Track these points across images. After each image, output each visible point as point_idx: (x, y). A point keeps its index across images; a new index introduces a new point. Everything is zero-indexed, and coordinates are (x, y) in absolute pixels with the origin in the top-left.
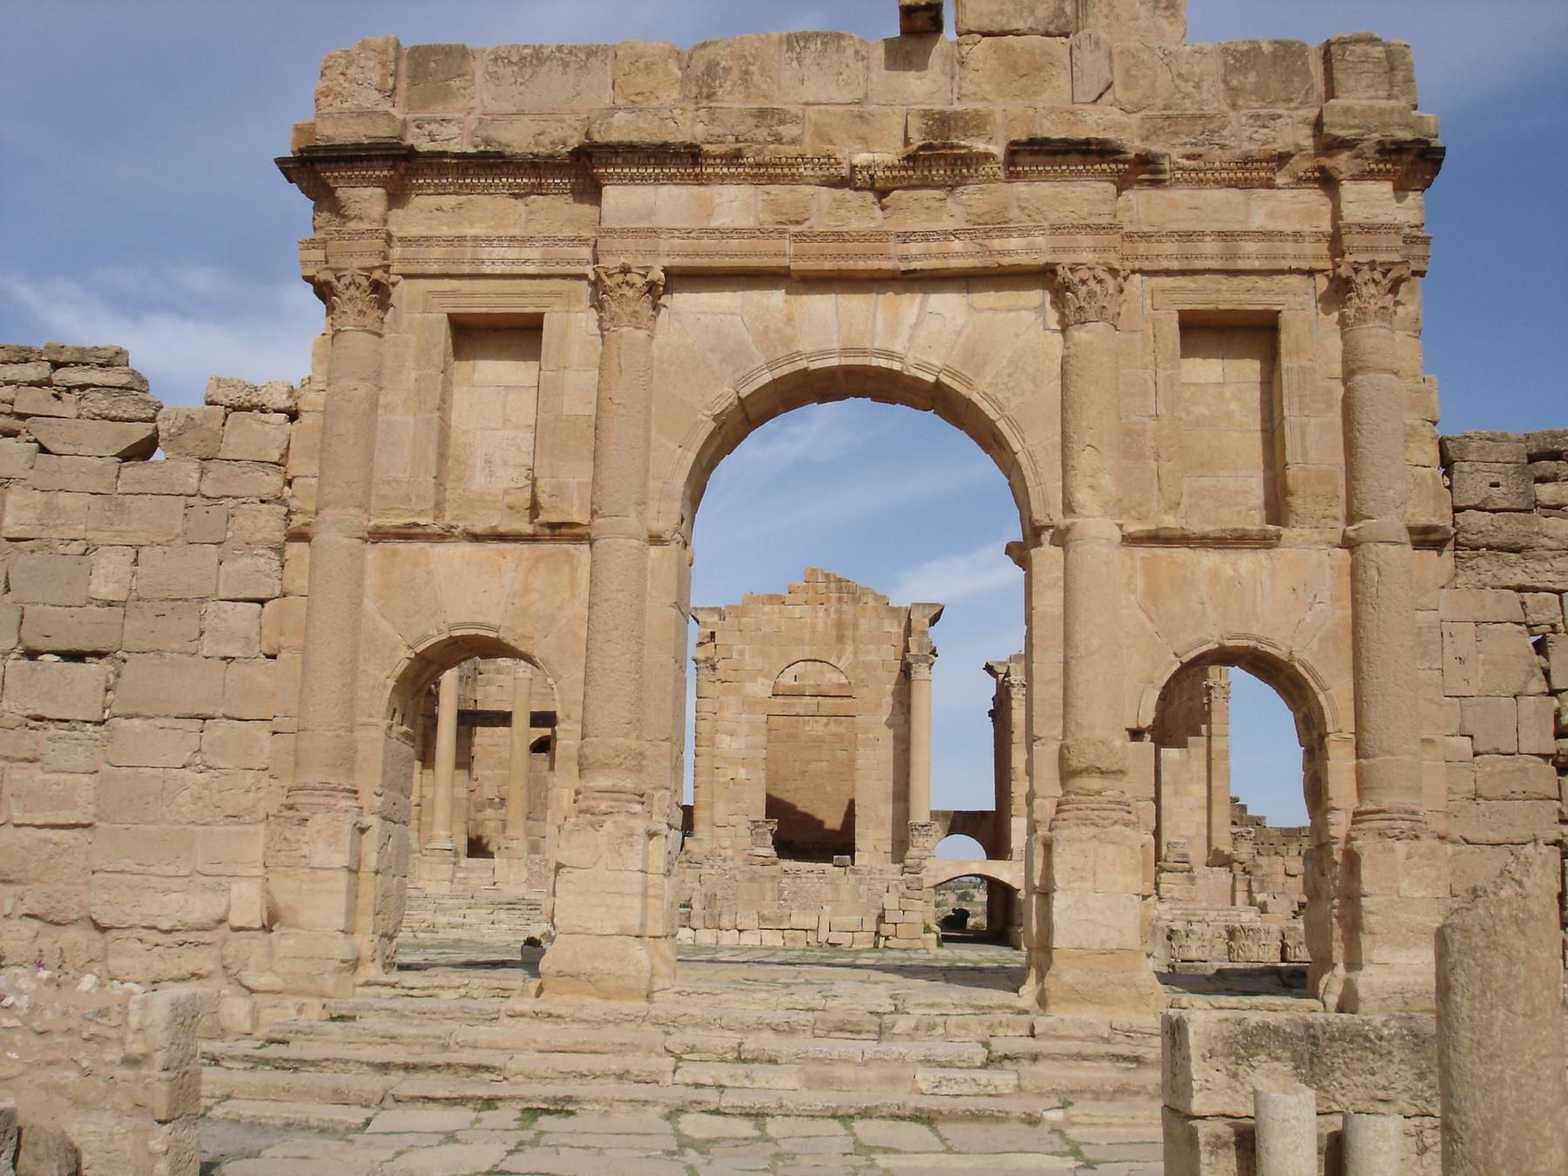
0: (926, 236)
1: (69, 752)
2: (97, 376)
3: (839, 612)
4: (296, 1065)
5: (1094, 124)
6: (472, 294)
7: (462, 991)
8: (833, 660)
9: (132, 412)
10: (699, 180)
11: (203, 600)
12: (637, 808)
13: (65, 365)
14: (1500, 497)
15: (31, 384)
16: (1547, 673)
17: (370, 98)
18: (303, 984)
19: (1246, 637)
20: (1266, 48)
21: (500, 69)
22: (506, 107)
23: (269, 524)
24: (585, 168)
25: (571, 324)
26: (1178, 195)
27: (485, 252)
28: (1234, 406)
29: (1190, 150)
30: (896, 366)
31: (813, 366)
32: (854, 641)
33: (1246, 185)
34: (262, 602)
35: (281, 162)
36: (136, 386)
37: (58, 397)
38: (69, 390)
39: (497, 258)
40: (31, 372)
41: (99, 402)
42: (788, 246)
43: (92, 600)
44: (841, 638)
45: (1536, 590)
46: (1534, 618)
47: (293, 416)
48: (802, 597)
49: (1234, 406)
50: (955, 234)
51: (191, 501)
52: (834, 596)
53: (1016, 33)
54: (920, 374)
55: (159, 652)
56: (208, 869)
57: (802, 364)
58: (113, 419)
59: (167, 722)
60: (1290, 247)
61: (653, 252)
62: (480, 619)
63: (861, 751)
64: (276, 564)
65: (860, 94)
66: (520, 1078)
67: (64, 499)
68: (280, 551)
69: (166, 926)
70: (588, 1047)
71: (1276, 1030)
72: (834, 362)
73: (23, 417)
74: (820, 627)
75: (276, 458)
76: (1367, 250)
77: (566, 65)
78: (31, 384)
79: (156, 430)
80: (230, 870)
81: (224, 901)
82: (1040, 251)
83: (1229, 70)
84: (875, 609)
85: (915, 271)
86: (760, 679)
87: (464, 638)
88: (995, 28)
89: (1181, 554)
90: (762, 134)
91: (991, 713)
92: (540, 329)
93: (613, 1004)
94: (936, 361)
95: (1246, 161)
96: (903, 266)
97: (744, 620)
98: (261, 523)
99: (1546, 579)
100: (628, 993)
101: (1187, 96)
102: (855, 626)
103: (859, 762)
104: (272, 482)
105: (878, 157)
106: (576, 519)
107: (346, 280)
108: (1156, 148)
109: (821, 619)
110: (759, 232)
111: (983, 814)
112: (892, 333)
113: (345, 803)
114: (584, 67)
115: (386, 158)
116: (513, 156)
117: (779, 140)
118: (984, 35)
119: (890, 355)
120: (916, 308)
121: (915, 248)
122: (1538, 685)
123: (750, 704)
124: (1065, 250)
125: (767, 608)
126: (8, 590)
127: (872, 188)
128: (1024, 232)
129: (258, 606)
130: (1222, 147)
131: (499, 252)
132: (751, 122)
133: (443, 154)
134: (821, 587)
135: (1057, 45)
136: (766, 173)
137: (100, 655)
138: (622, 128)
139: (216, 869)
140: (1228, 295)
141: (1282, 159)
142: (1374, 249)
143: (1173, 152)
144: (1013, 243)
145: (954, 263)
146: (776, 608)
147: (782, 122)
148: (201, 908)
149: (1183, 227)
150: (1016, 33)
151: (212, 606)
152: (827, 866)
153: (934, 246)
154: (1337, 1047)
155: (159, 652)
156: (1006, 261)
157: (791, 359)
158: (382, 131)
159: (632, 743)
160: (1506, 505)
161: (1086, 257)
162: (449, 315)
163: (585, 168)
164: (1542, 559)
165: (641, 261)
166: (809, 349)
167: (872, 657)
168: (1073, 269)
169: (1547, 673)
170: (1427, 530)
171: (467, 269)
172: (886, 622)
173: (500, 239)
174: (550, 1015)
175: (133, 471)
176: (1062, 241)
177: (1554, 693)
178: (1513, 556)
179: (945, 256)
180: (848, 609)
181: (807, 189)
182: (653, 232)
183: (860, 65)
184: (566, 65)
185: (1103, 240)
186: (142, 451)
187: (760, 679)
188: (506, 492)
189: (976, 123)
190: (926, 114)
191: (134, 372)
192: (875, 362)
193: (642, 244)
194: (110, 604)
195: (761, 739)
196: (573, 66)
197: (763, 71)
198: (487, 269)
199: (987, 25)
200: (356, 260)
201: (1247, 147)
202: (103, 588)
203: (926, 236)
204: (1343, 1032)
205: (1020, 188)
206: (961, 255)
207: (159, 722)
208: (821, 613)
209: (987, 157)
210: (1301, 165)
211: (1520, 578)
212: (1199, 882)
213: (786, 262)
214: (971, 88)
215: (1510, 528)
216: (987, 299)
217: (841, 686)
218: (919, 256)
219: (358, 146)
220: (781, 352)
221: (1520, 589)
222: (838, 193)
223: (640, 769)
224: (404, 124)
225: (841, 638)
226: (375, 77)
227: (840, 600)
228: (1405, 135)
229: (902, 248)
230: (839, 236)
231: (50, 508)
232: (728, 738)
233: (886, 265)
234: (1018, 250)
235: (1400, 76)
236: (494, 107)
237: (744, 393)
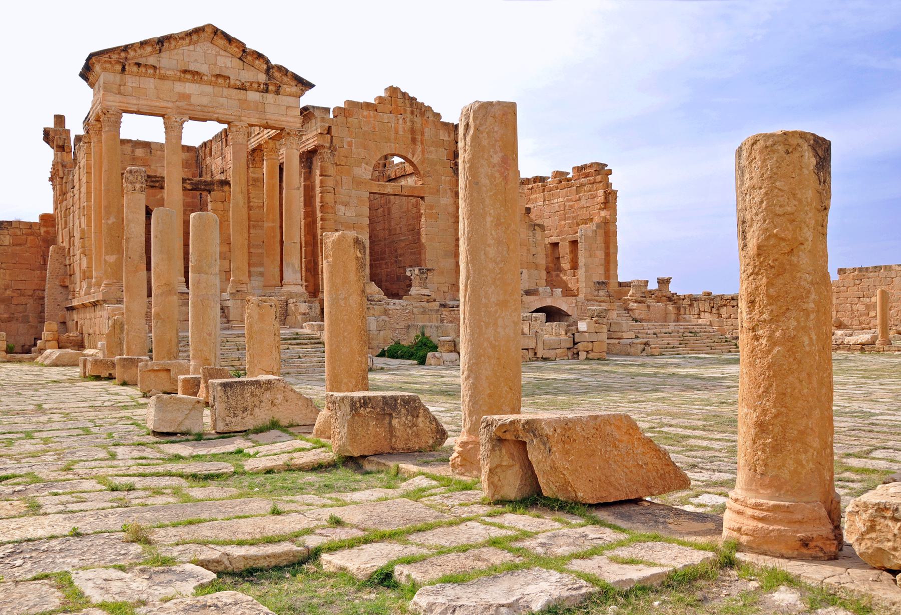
3: (412, 121)
8: (409, 156)
32: (422, 143)
48: (388, 107)
52: (409, 109)
74: (401, 133)
84: (434, 122)
86: (364, 165)
97: (350, 120)
102: (423, 134)
109: (401, 124)
123: (357, 183)
125: (365, 113)
146: (372, 113)
167: (433, 156)
172: (441, 132)
180: (418, 120)
187: (364, 165)
195: (366, 210)
208: (401, 121)
212: (651, 308)
225: (414, 140)
227: (412, 113)
232: (343, 208)
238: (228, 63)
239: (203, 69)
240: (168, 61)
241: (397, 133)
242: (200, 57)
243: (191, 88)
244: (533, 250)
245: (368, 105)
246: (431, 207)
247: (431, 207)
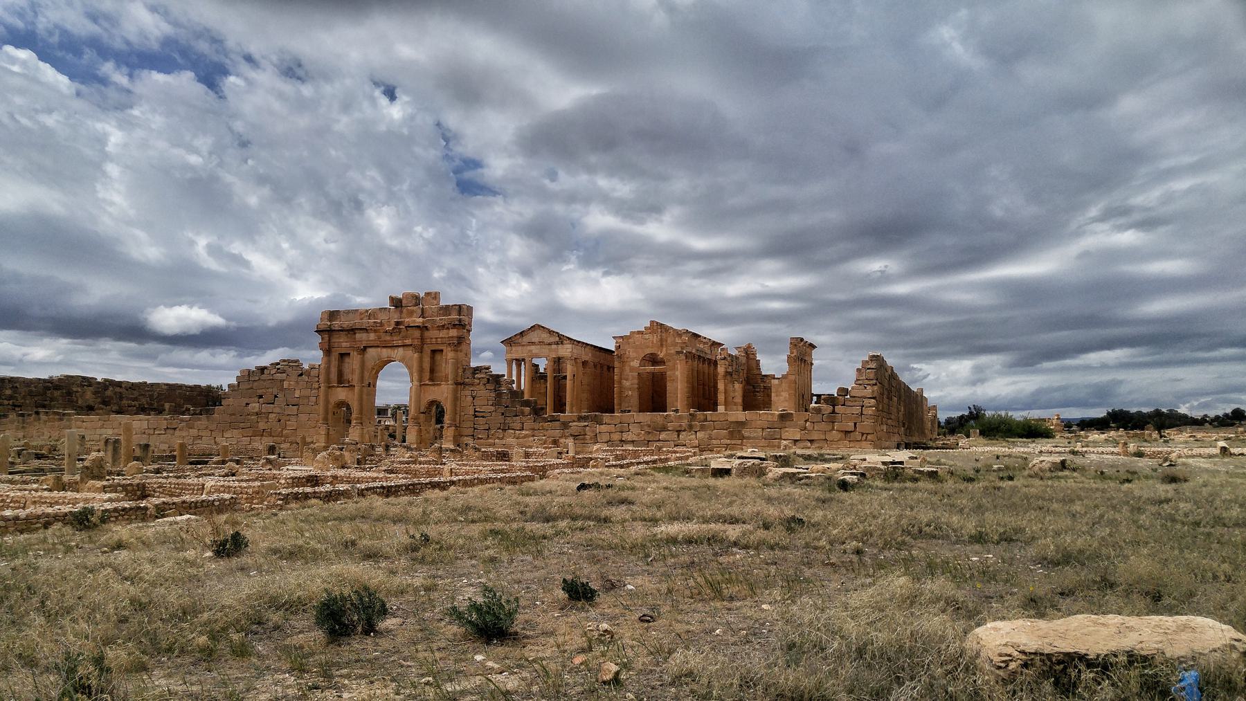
1: (293, 419)
25: (354, 354)
39: (344, 345)
109: (655, 339)
123: (632, 369)
136: (375, 331)
195: (636, 381)
206: (400, 343)
238: (545, 337)
239: (536, 340)
240: (525, 340)
242: (534, 337)
243: (533, 347)
245: (639, 332)
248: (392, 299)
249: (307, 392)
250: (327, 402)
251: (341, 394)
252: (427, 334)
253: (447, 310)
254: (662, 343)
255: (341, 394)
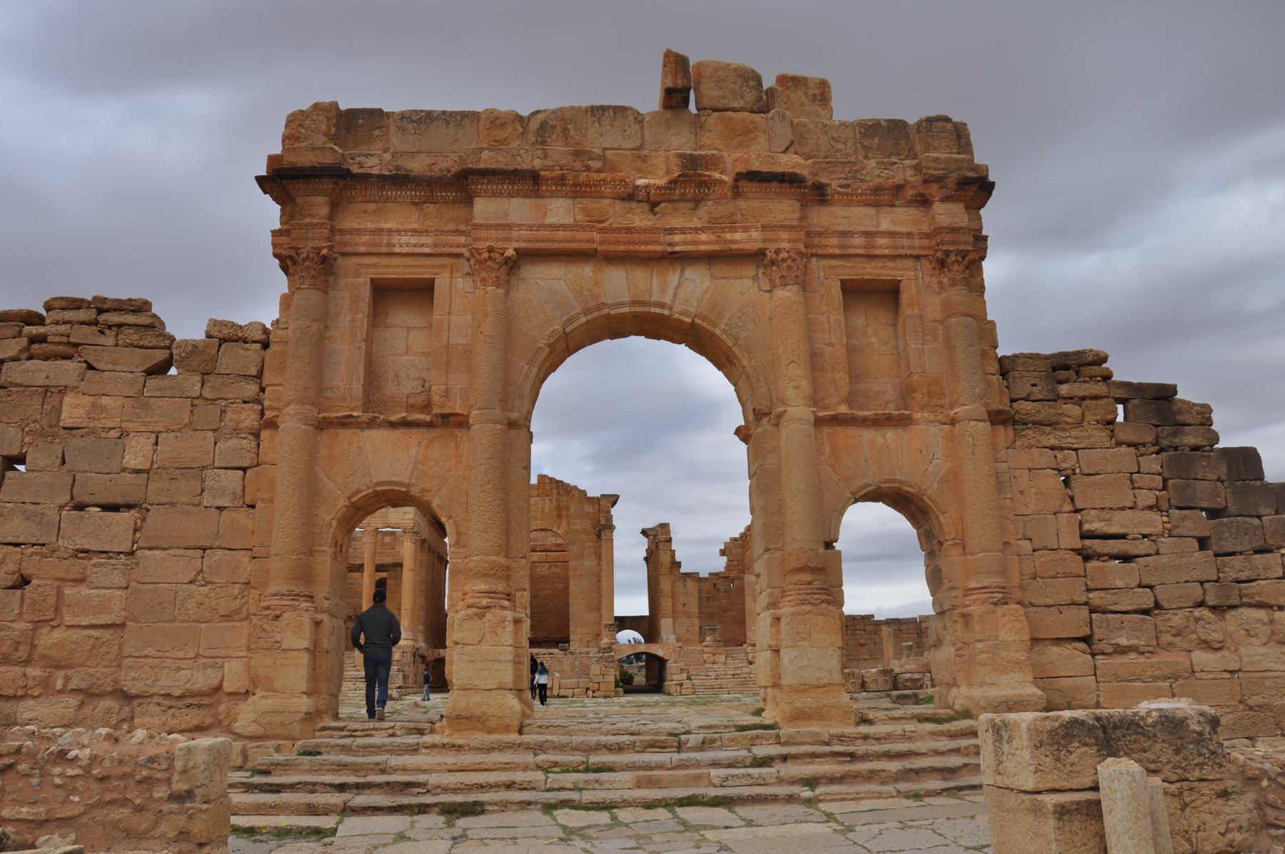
0: (683, 231)
1: (107, 574)
2: (130, 319)
3: (558, 500)
4: (277, 789)
5: (789, 162)
6: (387, 266)
7: (391, 731)
9: (154, 342)
10: (538, 195)
11: (203, 468)
12: (506, 603)
13: (107, 311)
14: (1038, 392)
15: (83, 323)
16: (1072, 499)
17: (320, 140)
18: (278, 731)
19: (893, 481)
20: (883, 123)
21: (405, 124)
22: (408, 148)
23: (249, 417)
24: (463, 184)
25: (454, 287)
26: (837, 210)
27: (395, 239)
28: (873, 339)
29: (843, 182)
30: (666, 312)
31: (612, 312)
33: (877, 205)
34: (244, 469)
35: (259, 179)
36: (155, 326)
37: (102, 332)
38: (110, 327)
39: (404, 243)
40: (82, 315)
41: (131, 336)
42: (596, 236)
43: (124, 470)
44: (559, 516)
45: (1062, 449)
46: (1064, 465)
47: (266, 345)
49: (873, 339)
50: (702, 230)
51: (196, 402)
53: (734, 110)
54: (681, 318)
55: (172, 504)
56: (208, 653)
57: (606, 311)
58: (141, 347)
59: (179, 552)
60: (905, 242)
61: (509, 240)
62: (394, 479)
63: (572, 583)
64: (254, 444)
65: (638, 143)
66: (439, 791)
67: (105, 401)
68: (257, 435)
69: (177, 692)
70: (482, 766)
71: (1082, 723)
72: (626, 310)
73: (76, 345)
75: (254, 373)
76: (953, 243)
77: (448, 123)
78: (83, 323)
79: (171, 354)
80: (223, 653)
81: (220, 675)
82: (755, 241)
83: (864, 136)
85: (677, 252)
87: (383, 492)
88: (720, 106)
89: (852, 431)
90: (578, 165)
91: (646, 559)
92: (432, 289)
93: (496, 737)
94: (692, 309)
95: (877, 190)
96: (669, 249)
98: (243, 416)
99: (1067, 442)
100: (506, 729)
101: (839, 150)
102: (568, 509)
103: (572, 588)
104: (251, 389)
105: (652, 182)
106: (459, 411)
107: (304, 255)
108: (823, 180)
110: (575, 227)
111: (642, 617)
112: (663, 292)
113: (304, 605)
114: (459, 124)
115: (331, 176)
116: (416, 176)
117: (588, 169)
118: (715, 110)
119: (662, 305)
120: (677, 277)
121: (677, 238)
122: (1068, 507)
124: (771, 241)
126: (64, 462)
127: (648, 201)
128: (746, 229)
129: (241, 472)
130: (862, 181)
131: (405, 239)
132: (570, 158)
133: (369, 175)
134: (547, 487)
135: (758, 118)
136: (578, 191)
137: (129, 507)
138: (487, 160)
139: (213, 653)
140: (869, 270)
141: (898, 188)
142: (957, 243)
143: (833, 181)
144: (739, 236)
145: (702, 248)
147: (591, 159)
148: (203, 680)
149: (841, 228)
150: (734, 110)
151: (209, 472)
152: (556, 651)
153: (689, 237)
154: (1119, 733)
155: (172, 504)
156: (734, 247)
157: (599, 308)
158: (328, 159)
159: (501, 560)
160: (1041, 397)
161: (785, 245)
162: (372, 280)
163: (463, 184)
164: (1064, 430)
165: (499, 245)
166: (610, 302)
168: (777, 252)
169: (1072, 499)
170: (998, 412)
171: (384, 250)
173: (405, 231)
174: (454, 746)
175: (153, 382)
176: (769, 235)
177: (1077, 511)
178: (1048, 429)
179: (695, 243)
180: (564, 499)
181: (607, 201)
182: (508, 226)
183: (638, 126)
184: (448, 123)
185: (794, 235)
186: (160, 369)
188: (409, 396)
189: (713, 162)
190: (681, 156)
191: (154, 316)
192: (653, 310)
193: (500, 234)
194: (138, 471)
196: (452, 124)
197: (576, 128)
198: (397, 250)
199: (715, 103)
200: (315, 241)
201: (877, 181)
202: (132, 461)
203: (683, 231)
204: (1121, 721)
205: (742, 204)
206: (706, 243)
207: (172, 552)
209: (721, 182)
210: (909, 193)
211: (1053, 442)
213: (595, 246)
214: (709, 142)
215: (1044, 411)
216: (721, 270)
217: (558, 545)
218: (680, 242)
219: (313, 168)
220: (592, 304)
221: (1052, 448)
222: (626, 204)
223: (508, 578)
224: (343, 156)
225: (559, 516)
226: (323, 127)
228: (971, 174)
229: (669, 238)
230: (629, 230)
231: (94, 406)
233: (659, 248)
234: (743, 239)
235: (963, 142)
236: (402, 148)
237: (568, 329)
241: (543, 511)
244: (683, 600)
246: (575, 570)
247: (575, 570)
248: (675, 63)
249: (195, 447)
250: (311, 494)
251: (386, 456)
252: (822, 217)
253: (890, 134)
254: (560, 512)
255: (386, 456)
